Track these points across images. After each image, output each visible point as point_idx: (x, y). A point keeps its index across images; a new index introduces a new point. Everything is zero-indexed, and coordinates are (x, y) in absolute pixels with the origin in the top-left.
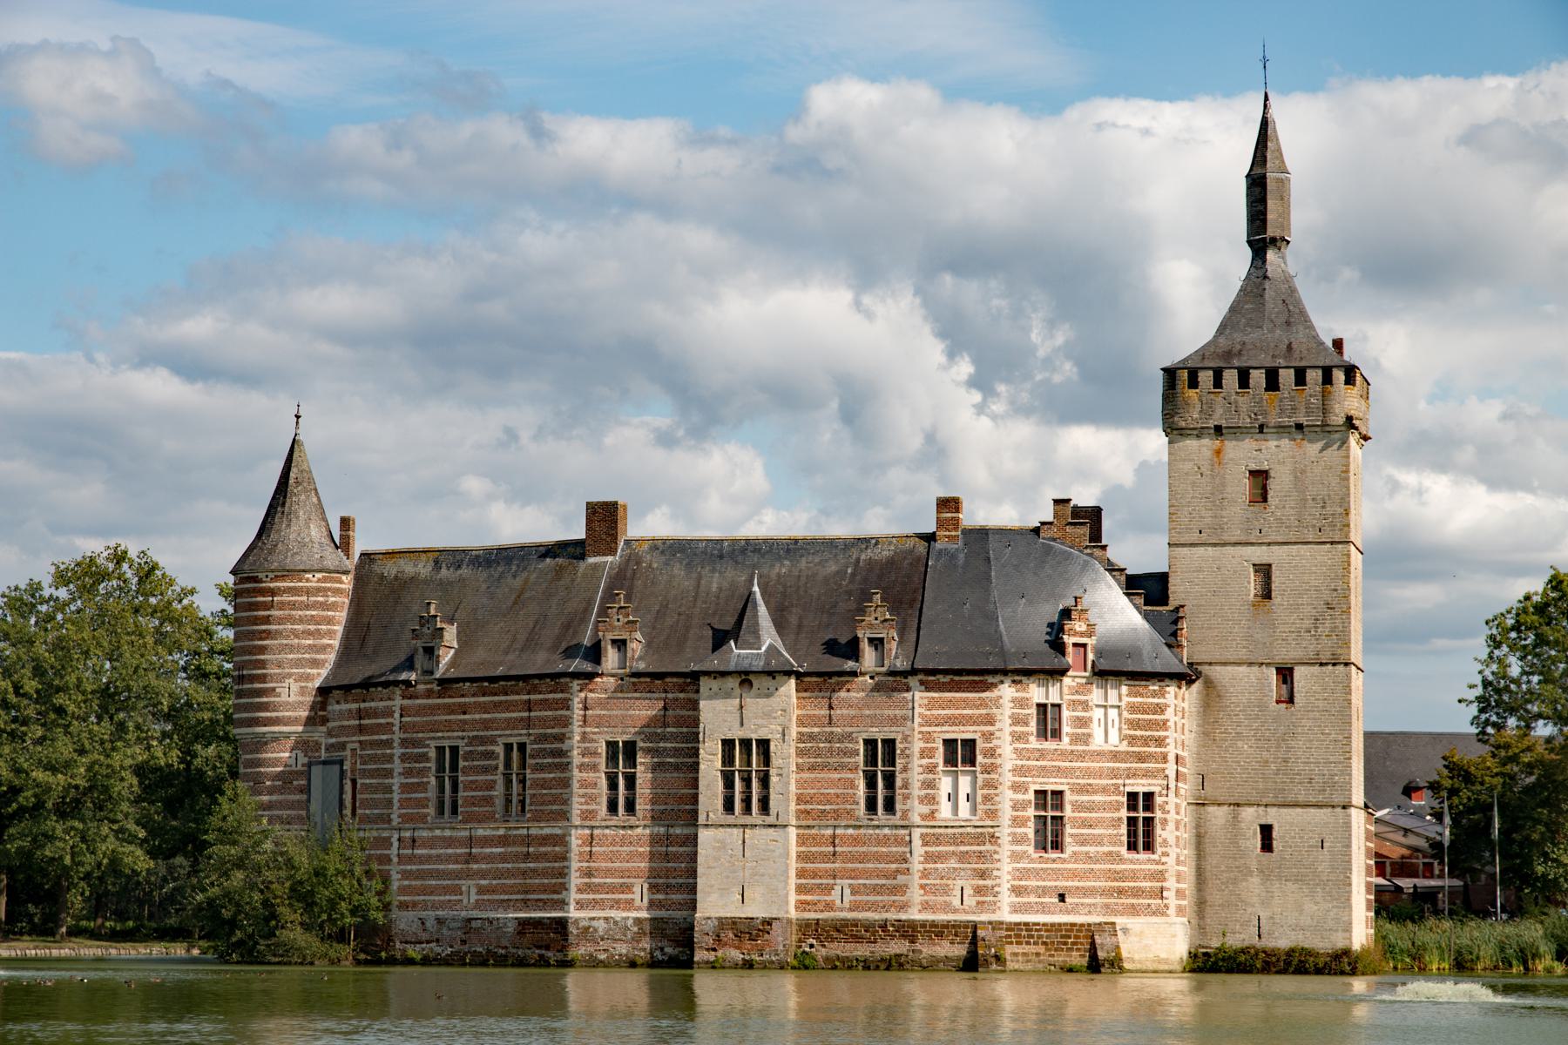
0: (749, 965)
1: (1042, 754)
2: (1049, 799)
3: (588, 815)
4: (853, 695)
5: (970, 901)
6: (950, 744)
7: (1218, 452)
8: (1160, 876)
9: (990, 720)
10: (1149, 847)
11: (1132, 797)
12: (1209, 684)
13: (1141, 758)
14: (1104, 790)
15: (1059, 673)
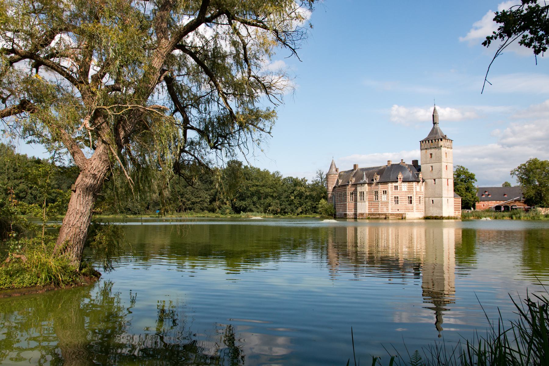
0: (362, 219)
1: (395, 192)
4: (373, 186)
8: (413, 207)
10: (411, 203)
11: (409, 197)
12: (426, 182)
13: (410, 192)
15: (397, 182)
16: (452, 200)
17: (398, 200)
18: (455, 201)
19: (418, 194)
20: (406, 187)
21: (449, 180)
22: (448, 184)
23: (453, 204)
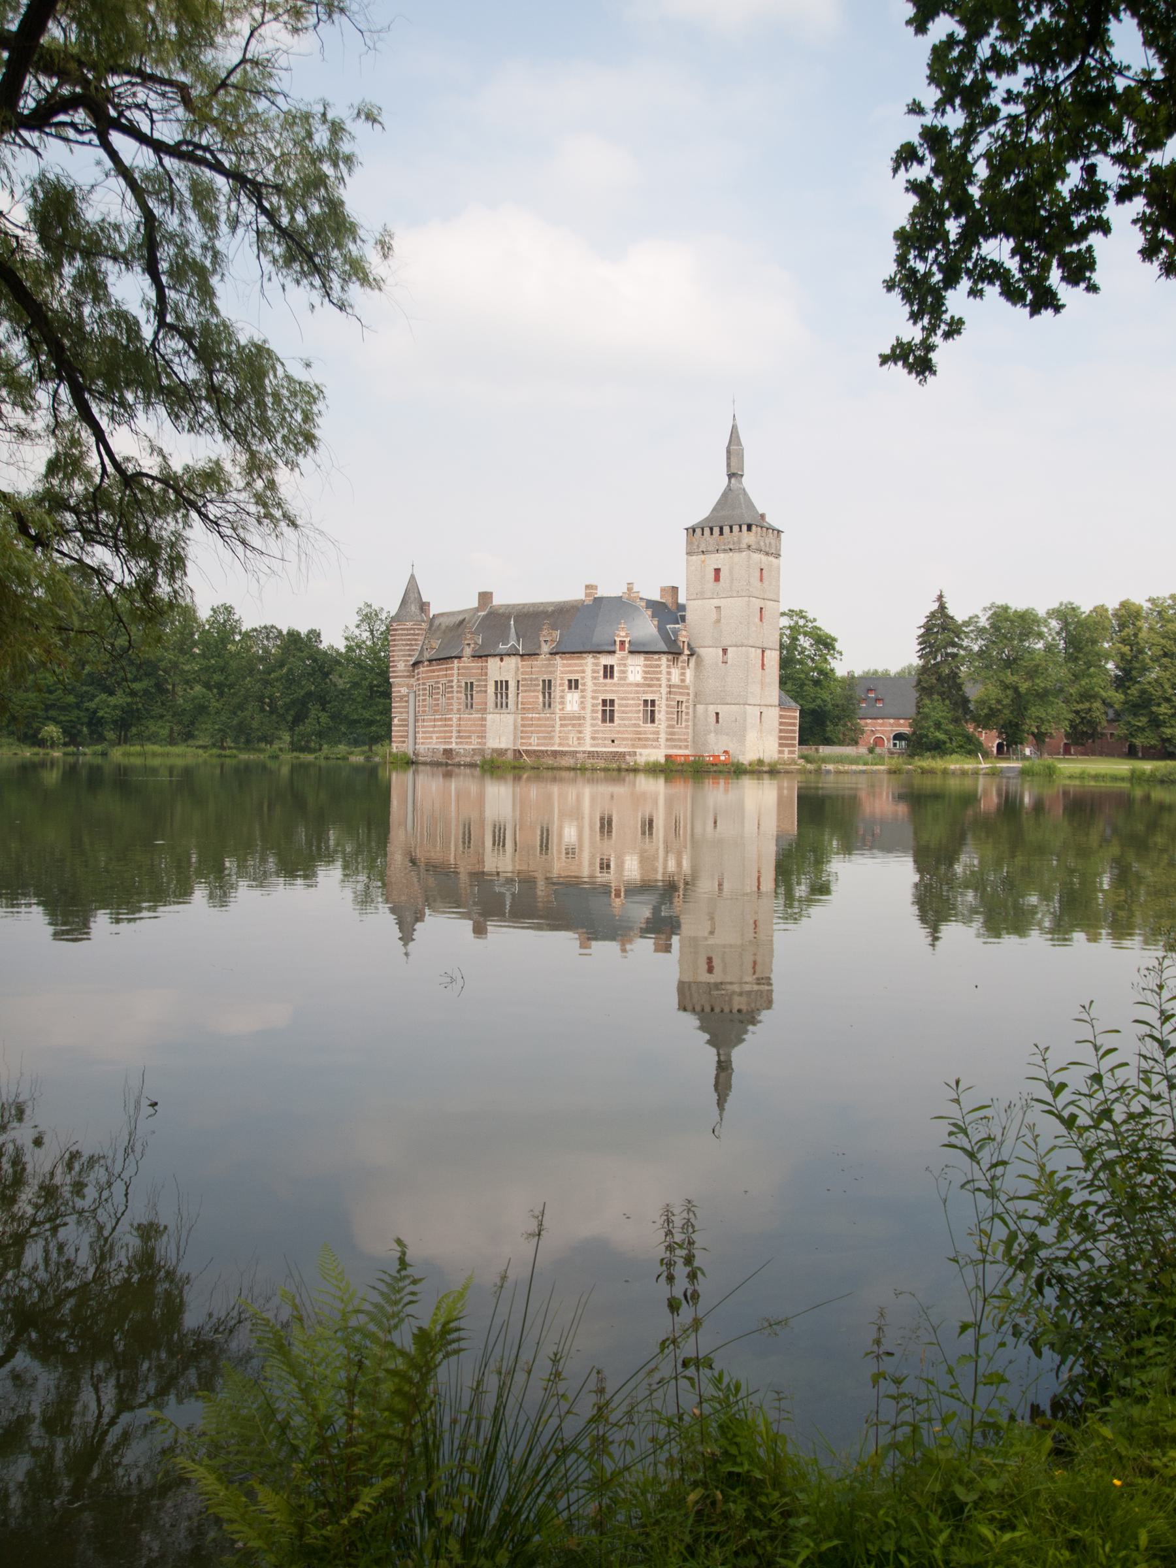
1: (605, 685)
2: (608, 703)
3: (459, 710)
5: (576, 743)
6: (570, 681)
7: (703, 562)
8: (658, 733)
9: (583, 672)
10: (653, 721)
11: (646, 701)
12: (698, 656)
14: (633, 699)
16: (773, 714)
17: (612, 711)
18: (781, 717)
19: (675, 693)
20: (638, 668)
21: (767, 653)
22: (763, 665)
23: (776, 724)
